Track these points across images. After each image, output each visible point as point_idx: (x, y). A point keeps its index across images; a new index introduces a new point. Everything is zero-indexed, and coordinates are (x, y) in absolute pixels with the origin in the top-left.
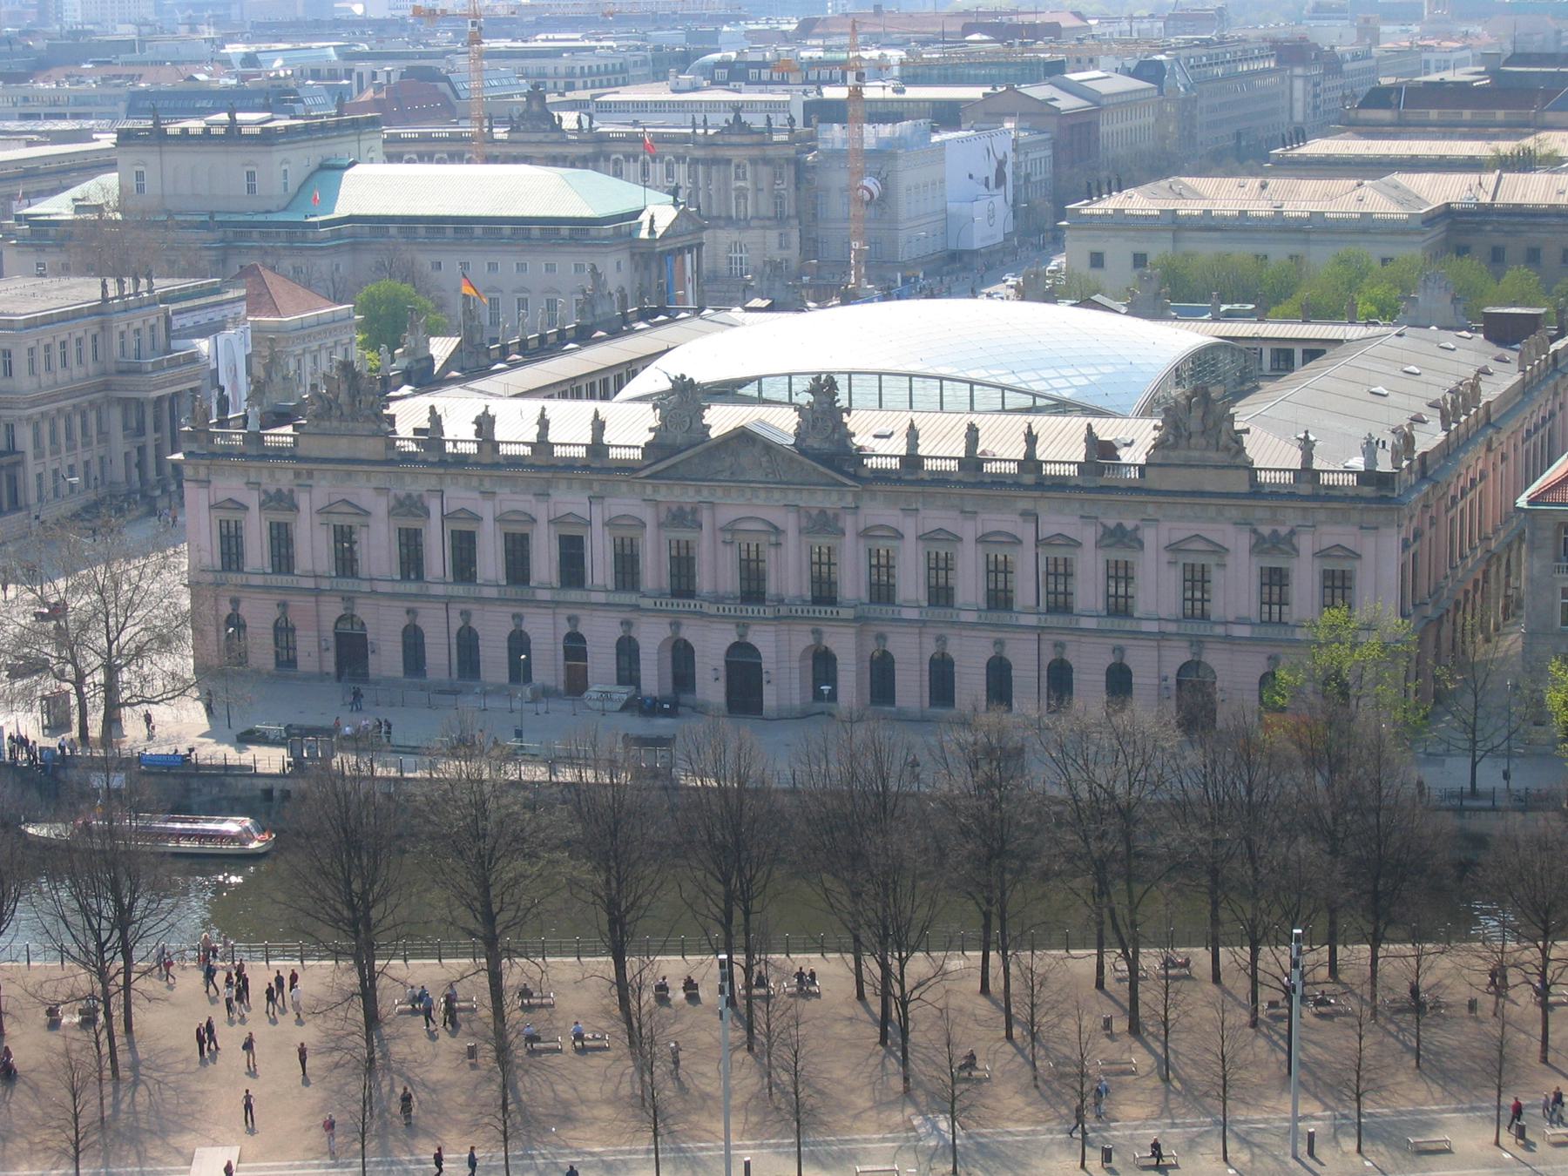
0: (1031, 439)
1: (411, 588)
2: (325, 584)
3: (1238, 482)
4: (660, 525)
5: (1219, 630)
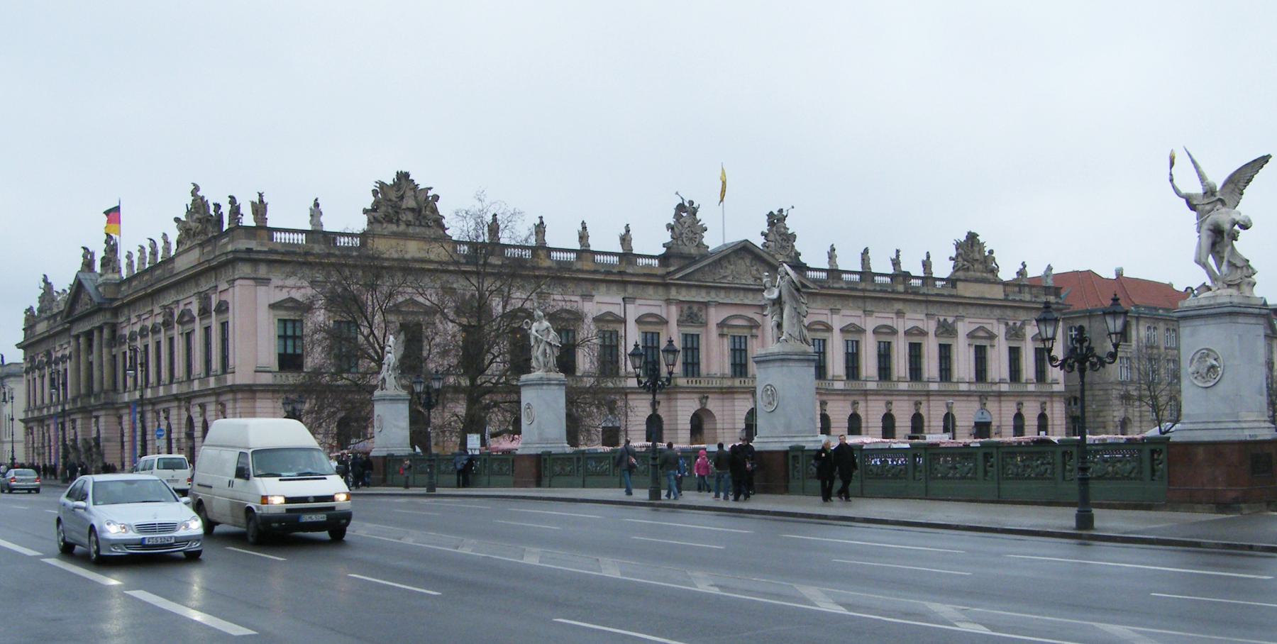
5: (995, 388)
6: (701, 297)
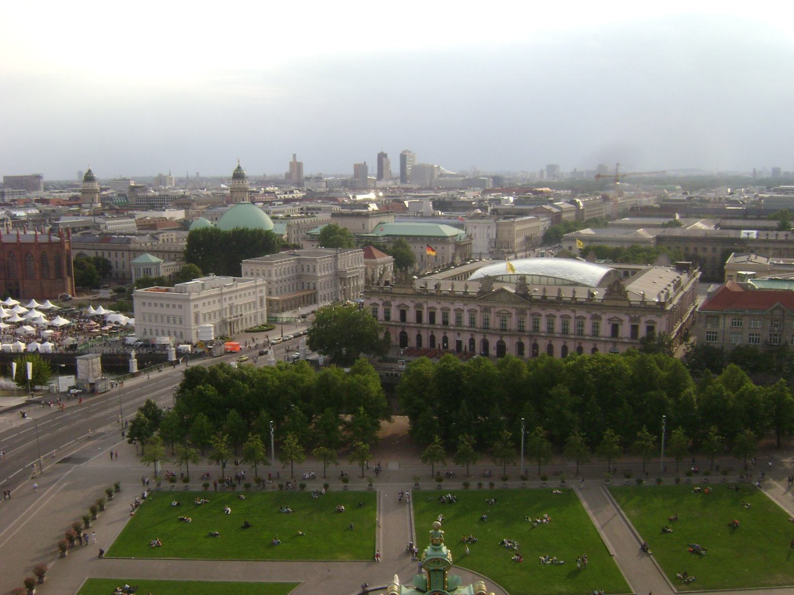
0: (574, 292)
1: (419, 325)
2: (398, 324)
3: (626, 304)
4: (481, 312)
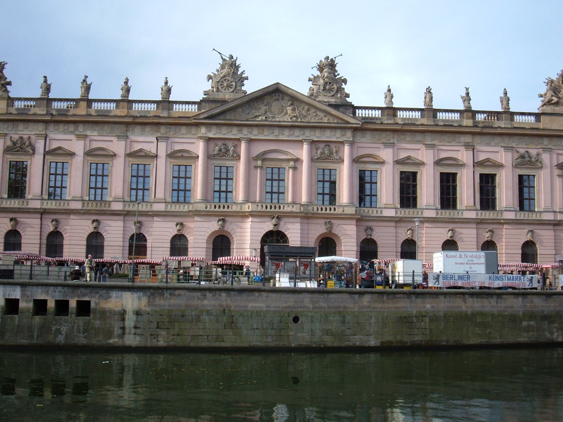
6: (234, 133)
